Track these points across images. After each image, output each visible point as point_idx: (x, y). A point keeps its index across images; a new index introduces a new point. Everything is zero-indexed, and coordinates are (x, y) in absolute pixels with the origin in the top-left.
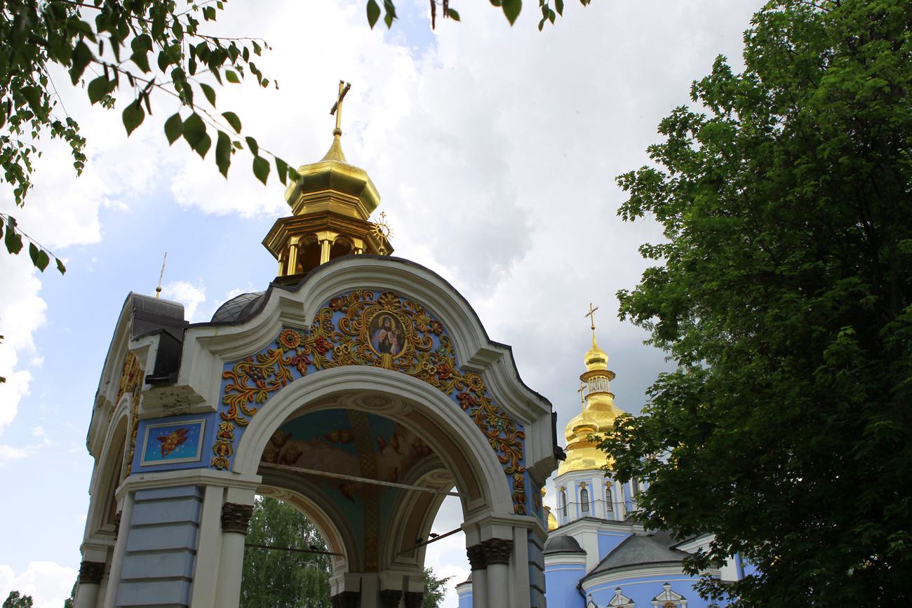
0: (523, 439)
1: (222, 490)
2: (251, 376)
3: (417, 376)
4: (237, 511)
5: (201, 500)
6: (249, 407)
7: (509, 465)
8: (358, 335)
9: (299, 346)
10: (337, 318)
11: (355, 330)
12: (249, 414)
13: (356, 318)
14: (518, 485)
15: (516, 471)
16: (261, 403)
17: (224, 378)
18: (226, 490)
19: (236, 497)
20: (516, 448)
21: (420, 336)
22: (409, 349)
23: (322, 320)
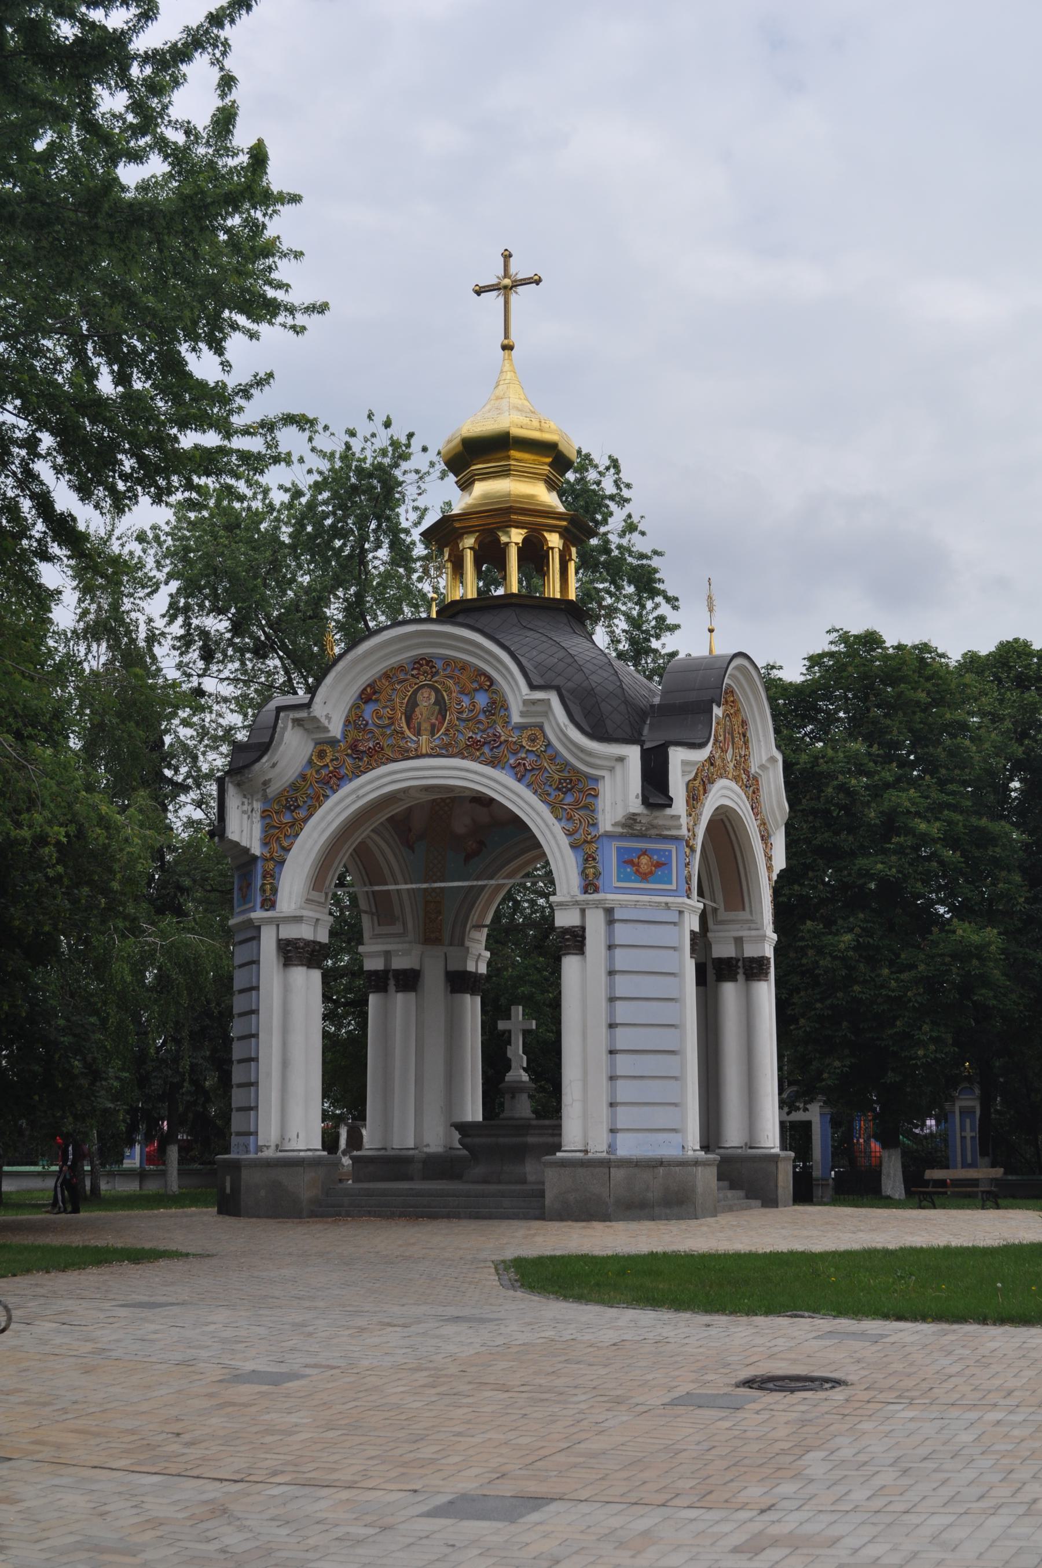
0: (596, 796)
1: (274, 927)
2: (288, 808)
3: (460, 755)
4: (288, 945)
5: (259, 937)
6: (285, 844)
7: (577, 836)
8: (393, 724)
9: (332, 760)
10: (369, 710)
11: (389, 718)
12: (287, 850)
13: (388, 704)
14: (589, 859)
15: (586, 842)
16: (297, 835)
17: (263, 818)
18: (278, 926)
19: (289, 932)
20: (588, 812)
21: (466, 702)
22: (450, 721)
23: (353, 721)
